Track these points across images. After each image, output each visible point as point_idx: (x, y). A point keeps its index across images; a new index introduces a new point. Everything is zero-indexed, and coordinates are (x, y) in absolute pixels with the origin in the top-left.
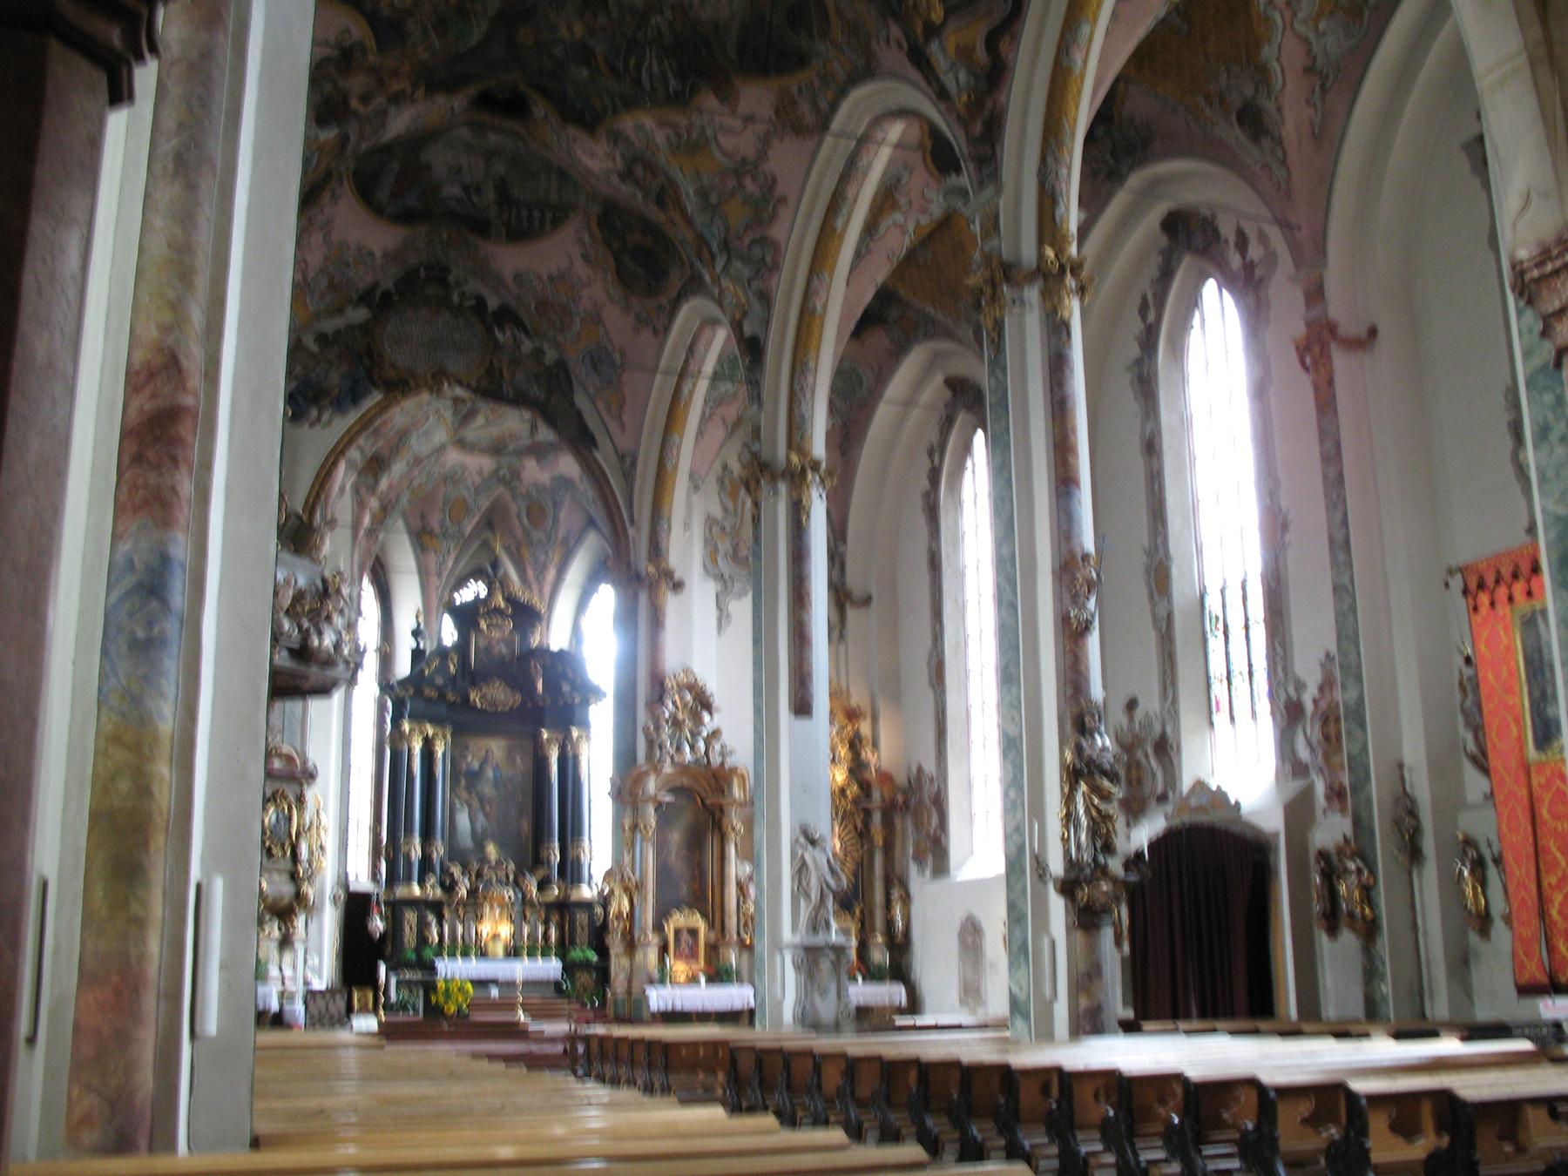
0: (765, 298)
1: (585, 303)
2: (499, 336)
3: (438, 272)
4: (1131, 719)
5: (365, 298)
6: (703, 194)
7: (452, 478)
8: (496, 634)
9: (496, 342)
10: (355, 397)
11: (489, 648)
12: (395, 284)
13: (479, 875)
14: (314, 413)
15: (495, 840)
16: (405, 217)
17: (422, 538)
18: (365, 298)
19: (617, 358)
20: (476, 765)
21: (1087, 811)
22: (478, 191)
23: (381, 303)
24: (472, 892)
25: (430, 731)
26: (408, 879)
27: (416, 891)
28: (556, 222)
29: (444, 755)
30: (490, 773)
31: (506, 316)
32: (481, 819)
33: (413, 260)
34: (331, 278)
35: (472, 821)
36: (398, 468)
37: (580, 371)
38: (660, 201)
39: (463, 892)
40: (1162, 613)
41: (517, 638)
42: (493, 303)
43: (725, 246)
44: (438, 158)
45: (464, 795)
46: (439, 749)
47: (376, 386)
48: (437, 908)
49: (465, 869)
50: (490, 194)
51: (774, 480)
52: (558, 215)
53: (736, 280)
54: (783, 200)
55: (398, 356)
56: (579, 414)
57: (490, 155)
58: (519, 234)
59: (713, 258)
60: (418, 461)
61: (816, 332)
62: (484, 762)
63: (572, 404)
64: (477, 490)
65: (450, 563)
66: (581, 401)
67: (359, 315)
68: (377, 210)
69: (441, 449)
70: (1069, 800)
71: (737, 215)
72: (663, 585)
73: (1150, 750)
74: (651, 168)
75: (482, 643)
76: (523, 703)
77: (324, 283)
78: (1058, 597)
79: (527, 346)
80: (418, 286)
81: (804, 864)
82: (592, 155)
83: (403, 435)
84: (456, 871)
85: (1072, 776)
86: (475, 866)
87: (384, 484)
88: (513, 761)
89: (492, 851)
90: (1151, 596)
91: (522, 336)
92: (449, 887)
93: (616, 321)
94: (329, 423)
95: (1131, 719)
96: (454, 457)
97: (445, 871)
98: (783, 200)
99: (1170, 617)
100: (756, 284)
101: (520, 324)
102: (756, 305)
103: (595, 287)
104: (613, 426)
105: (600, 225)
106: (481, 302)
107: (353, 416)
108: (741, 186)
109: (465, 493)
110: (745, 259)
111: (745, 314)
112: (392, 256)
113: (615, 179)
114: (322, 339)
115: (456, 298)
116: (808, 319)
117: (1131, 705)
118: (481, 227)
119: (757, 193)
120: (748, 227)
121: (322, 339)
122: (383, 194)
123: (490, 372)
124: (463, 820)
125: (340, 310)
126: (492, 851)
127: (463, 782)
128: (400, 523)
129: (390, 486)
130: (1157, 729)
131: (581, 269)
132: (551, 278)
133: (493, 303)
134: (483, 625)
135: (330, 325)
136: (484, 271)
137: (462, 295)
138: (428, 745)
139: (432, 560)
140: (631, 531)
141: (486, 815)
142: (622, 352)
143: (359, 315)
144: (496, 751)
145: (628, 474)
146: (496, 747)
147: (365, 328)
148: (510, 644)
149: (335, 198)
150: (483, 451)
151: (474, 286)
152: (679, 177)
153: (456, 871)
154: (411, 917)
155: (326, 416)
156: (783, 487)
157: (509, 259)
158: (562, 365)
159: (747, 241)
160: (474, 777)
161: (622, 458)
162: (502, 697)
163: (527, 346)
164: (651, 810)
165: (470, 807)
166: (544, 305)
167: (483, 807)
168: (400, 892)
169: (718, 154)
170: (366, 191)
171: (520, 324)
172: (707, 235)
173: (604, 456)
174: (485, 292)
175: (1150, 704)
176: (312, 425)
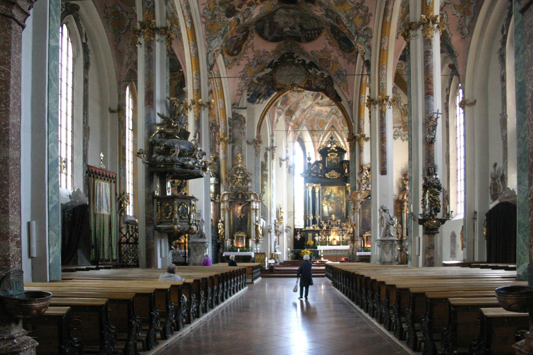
0: (369, 47)
1: (333, 58)
2: (310, 71)
3: (291, 55)
4: (495, 170)
5: (270, 66)
6: (348, 17)
7: (319, 114)
8: (333, 157)
9: (309, 73)
10: (269, 95)
11: (331, 161)
12: (278, 60)
13: (330, 223)
14: (258, 100)
15: (334, 214)
16: (275, 40)
17: (312, 132)
18: (270, 66)
19: (344, 73)
20: (329, 194)
21: (429, 198)
22: (294, 28)
23: (274, 66)
24: (327, 228)
25: (315, 185)
26: (309, 226)
27: (311, 228)
28: (319, 34)
29: (319, 191)
30: (333, 196)
31: (312, 65)
32: (331, 209)
33: (283, 52)
34: (257, 61)
35: (328, 209)
36: (298, 113)
37: (335, 78)
38: (337, 23)
39: (325, 228)
40: (504, 135)
41: (339, 158)
42: (308, 62)
43: (356, 33)
44: (279, 20)
45: (326, 202)
46: (317, 190)
47: (275, 91)
48: (318, 232)
49: (326, 222)
50: (298, 29)
51: (374, 104)
52: (319, 32)
53: (361, 43)
54: (371, 15)
55: (280, 81)
56: (336, 91)
57: (294, 16)
58: (310, 40)
59: (353, 37)
60: (304, 111)
61: (385, 56)
62: (331, 192)
63: (333, 88)
64: (327, 117)
65: (321, 138)
66: (336, 87)
67: (269, 70)
68: (266, 39)
69: (311, 106)
70: (424, 195)
71: (358, 22)
72: (362, 139)
73: (499, 179)
74: (332, 11)
75: (329, 160)
76: (341, 176)
77: (255, 63)
78: (424, 132)
79: (319, 73)
80: (284, 60)
81: (382, 217)
82: (316, 11)
83: (297, 103)
84: (323, 222)
85: (425, 188)
86: (329, 221)
87: (294, 118)
88: (339, 193)
89: (333, 217)
90: (502, 129)
91: (317, 70)
92: (321, 227)
93: (341, 61)
94: (262, 103)
95: (495, 170)
96: (317, 108)
97: (320, 223)
98: (371, 15)
99: (506, 135)
100: (367, 43)
101: (316, 67)
102: (368, 50)
103: (335, 53)
104: (346, 93)
105: (332, 33)
106: (304, 61)
107: (269, 100)
108: (358, 12)
109: (323, 118)
110: (363, 36)
111: (364, 53)
112: (276, 52)
113: (324, 17)
114: (259, 79)
115: (296, 62)
116: (383, 53)
117: (495, 165)
118: (299, 39)
119: (363, 14)
120: (362, 26)
121: (259, 79)
122: (266, 33)
123: (308, 82)
124: (325, 209)
125: (263, 70)
126: (333, 217)
128: (305, 128)
129: (296, 118)
130: (502, 172)
131: (330, 48)
132: (321, 51)
133: (308, 62)
134: (329, 155)
135: (260, 75)
136: (304, 53)
137: (299, 61)
138: (314, 188)
139: (316, 138)
140: (353, 124)
141: (332, 208)
142: (346, 71)
143: (269, 70)
145: (351, 108)
146: (334, 189)
147: (271, 74)
148: (337, 160)
149: (252, 37)
150: (325, 106)
151: (302, 57)
152: (340, 13)
153: (323, 222)
154: (310, 235)
155: (261, 101)
156: (377, 106)
157: (308, 47)
158: (329, 77)
159: (362, 30)
161: (349, 103)
162: (334, 175)
163: (319, 73)
164: (359, 204)
166: (321, 60)
168: (307, 228)
169: (350, 4)
170: (261, 34)
171: (316, 67)
172: (350, 30)
173: (344, 103)
174: (305, 58)
175: (500, 165)
176: (258, 103)
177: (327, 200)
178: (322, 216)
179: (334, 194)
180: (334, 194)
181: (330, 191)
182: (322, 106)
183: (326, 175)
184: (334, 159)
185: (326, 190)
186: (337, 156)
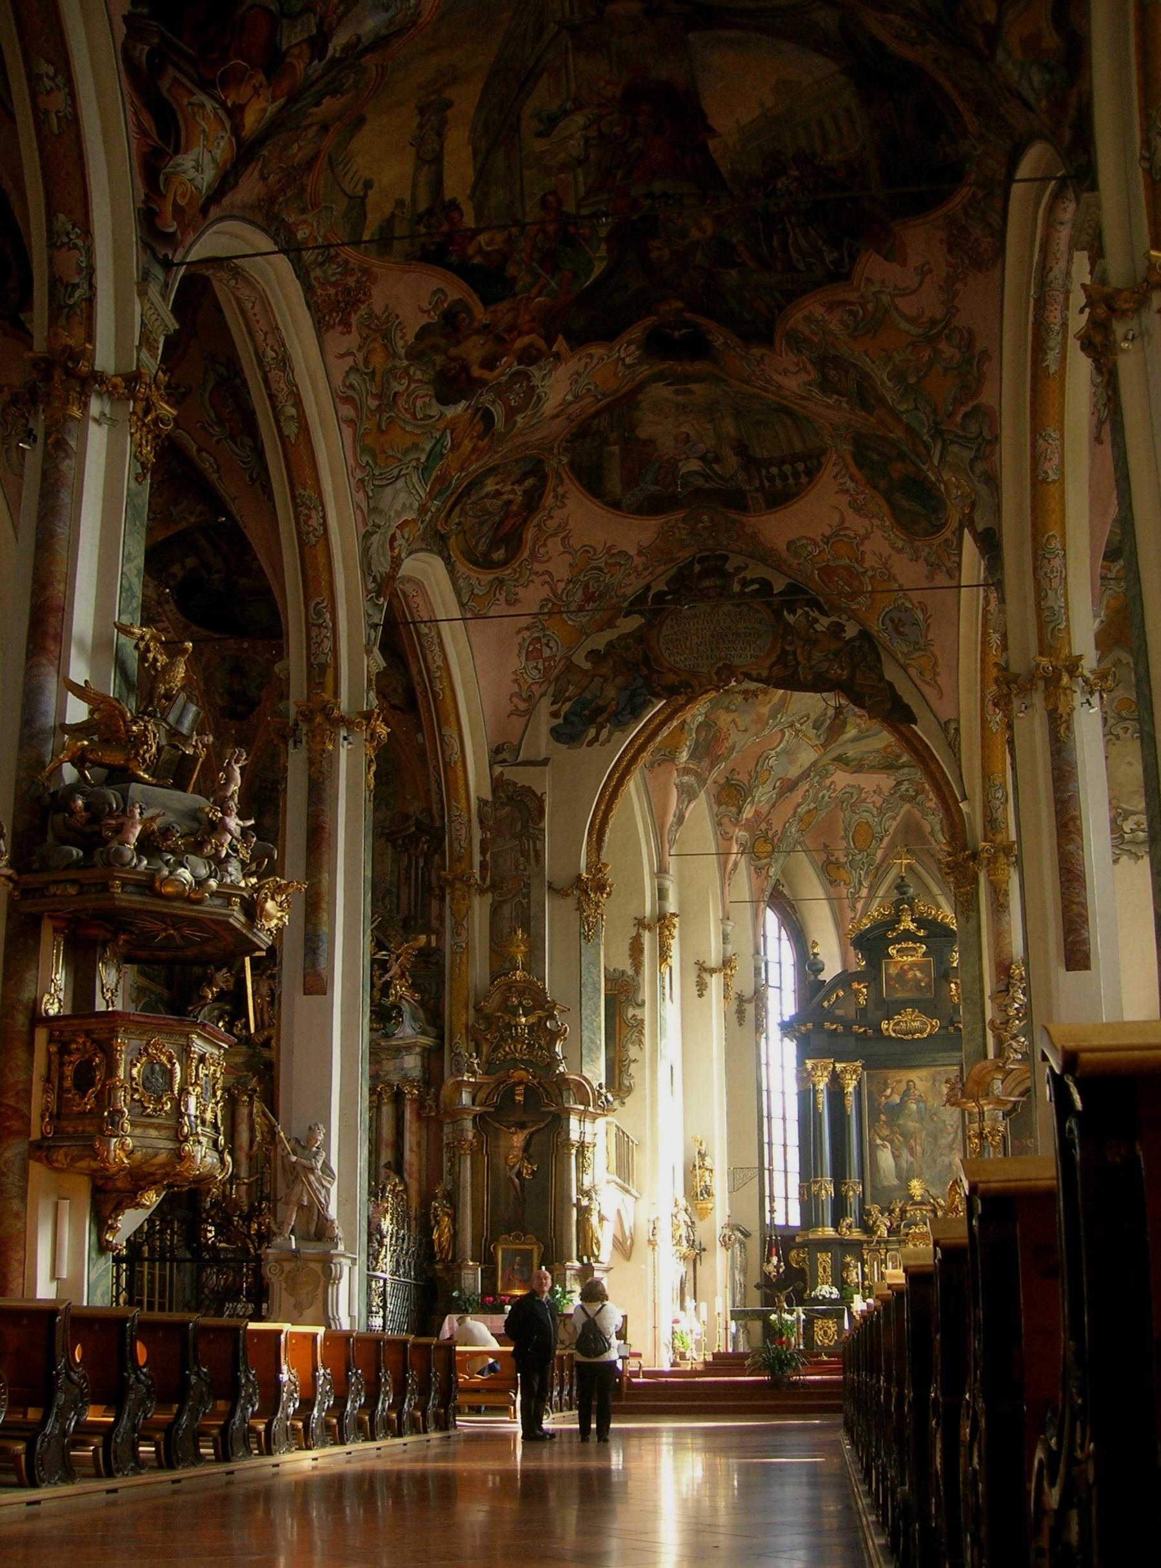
11: (902, 973)
13: (903, 1211)
20: (897, 1099)
35: (896, 1157)
45: (885, 1132)
62: (906, 1093)
75: (893, 971)
84: (875, 1209)
96: (841, 779)
97: (864, 1213)
124: (886, 1158)
127: (883, 1117)
134: (892, 951)
144: (917, 1082)
150: (873, 769)
160: (896, 1111)
165: (891, 1142)
167: (906, 1141)
177: (890, 1123)
178: (873, 1186)
179: (920, 1100)
180: (920, 1100)
181: (903, 1086)
182: (859, 769)
183: (884, 1026)
184: (913, 965)
185: (886, 1086)
186: (924, 955)
